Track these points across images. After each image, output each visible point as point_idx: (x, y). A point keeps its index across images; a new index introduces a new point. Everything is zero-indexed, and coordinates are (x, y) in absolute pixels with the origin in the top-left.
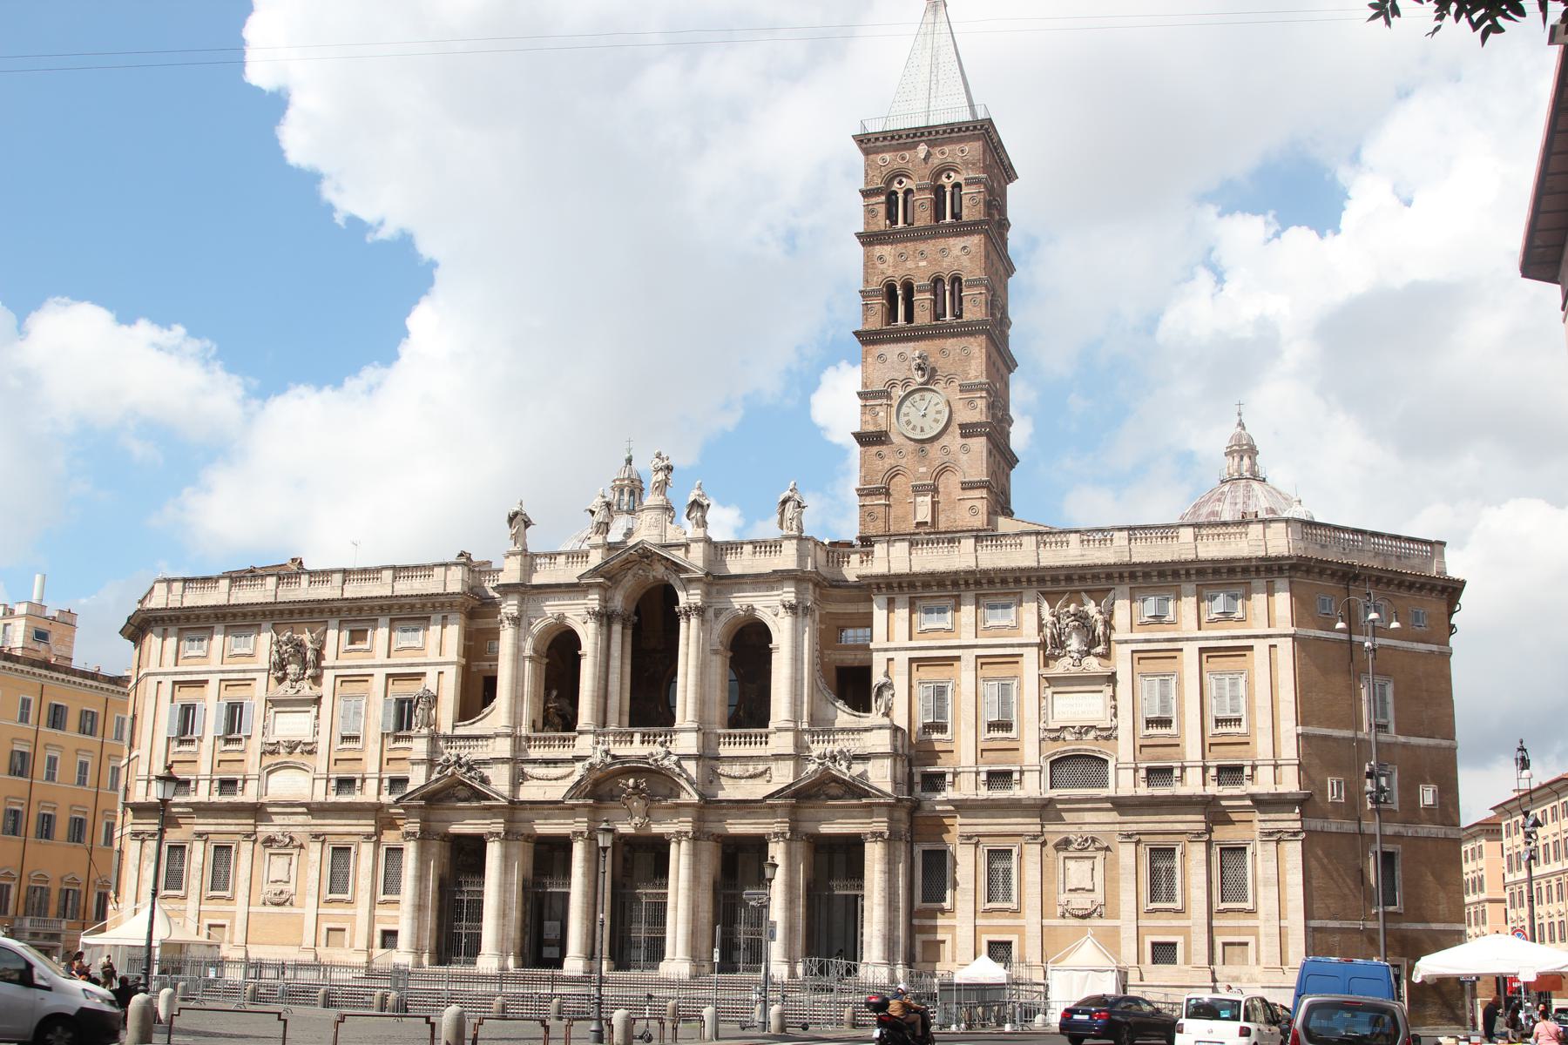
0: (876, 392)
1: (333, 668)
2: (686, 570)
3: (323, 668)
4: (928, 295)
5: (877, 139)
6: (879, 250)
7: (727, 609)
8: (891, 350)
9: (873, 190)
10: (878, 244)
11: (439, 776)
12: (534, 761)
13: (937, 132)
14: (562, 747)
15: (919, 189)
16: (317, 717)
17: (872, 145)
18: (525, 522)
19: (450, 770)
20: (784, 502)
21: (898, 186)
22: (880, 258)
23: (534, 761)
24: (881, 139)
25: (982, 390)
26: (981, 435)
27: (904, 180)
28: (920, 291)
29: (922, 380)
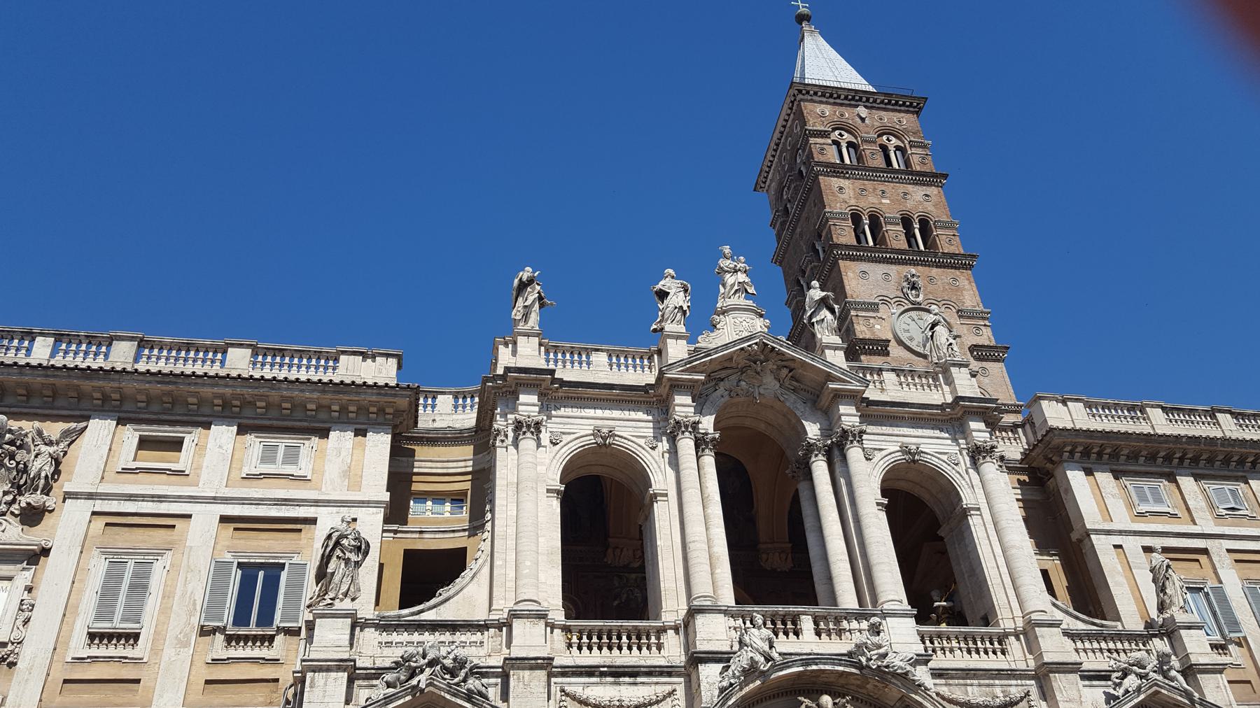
0: (869, 303)
1: (91, 496)
2: (830, 377)
3: (68, 496)
4: (900, 228)
5: (816, 93)
6: (836, 182)
7: (882, 449)
8: (877, 270)
9: (821, 131)
10: (834, 177)
11: (391, 690)
12: (589, 671)
13: (875, 101)
14: (635, 648)
15: (865, 141)
16: (29, 589)
17: (809, 98)
18: (540, 298)
19: (422, 679)
20: (934, 325)
21: (839, 137)
22: (841, 188)
23: (589, 671)
24: (820, 94)
25: (984, 319)
26: (998, 361)
27: (843, 132)
28: (891, 224)
29: (918, 300)
